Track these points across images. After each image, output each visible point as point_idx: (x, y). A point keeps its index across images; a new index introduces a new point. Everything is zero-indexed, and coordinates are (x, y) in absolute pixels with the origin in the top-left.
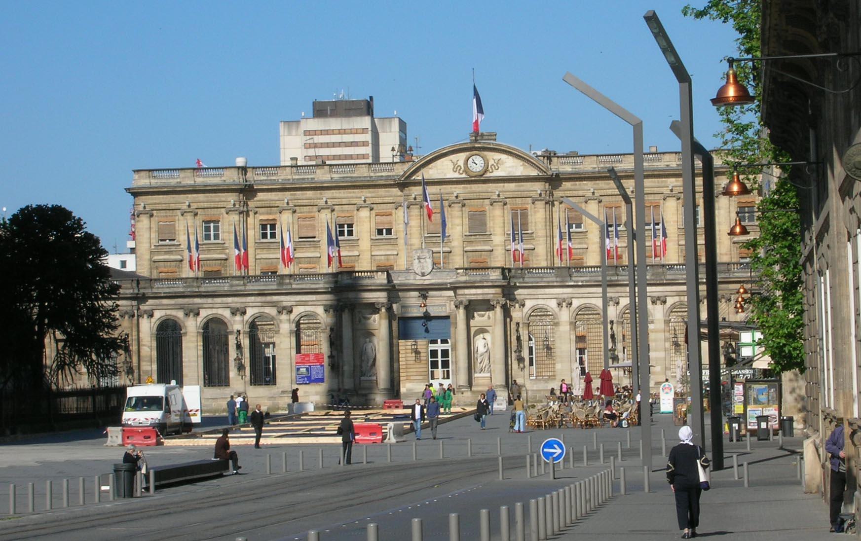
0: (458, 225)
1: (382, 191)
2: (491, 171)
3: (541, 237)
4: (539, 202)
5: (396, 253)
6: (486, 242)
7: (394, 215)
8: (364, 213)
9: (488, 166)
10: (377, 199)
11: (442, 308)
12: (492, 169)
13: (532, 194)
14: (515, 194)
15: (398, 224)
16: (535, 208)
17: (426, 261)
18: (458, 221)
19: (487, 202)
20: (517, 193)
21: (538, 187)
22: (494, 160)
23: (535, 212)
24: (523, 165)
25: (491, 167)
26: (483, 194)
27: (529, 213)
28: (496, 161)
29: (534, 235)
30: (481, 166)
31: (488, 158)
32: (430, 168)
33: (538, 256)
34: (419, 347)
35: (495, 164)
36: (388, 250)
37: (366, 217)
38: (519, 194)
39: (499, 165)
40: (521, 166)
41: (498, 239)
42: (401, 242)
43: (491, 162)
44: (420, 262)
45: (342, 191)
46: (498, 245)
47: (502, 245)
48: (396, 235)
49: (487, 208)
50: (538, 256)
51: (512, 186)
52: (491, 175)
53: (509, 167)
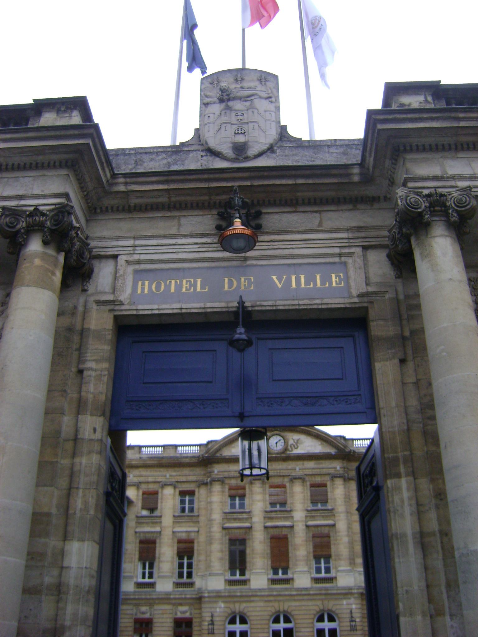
0: (259, 501)
1: (186, 471)
2: (290, 449)
3: (341, 513)
4: (338, 479)
5: (196, 529)
6: (286, 519)
7: (196, 493)
8: (168, 491)
9: (288, 444)
10: (181, 477)
11: (326, 278)
12: (292, 448)
13: (332, 471)
14: (314, 472)
15: (201, 502)
16: (334, 484)
17: (252, 107)
18: (258, 497)
19: (286, 480)
20: (316, 470)
21: (337, 466)
22: (294, 440)
23: (333, 488)
24: (322, 444)
25: (291, 446)
26: (284, 471)
27: (329, 490)
28: (296, 441)
29: (334, 511)
30: (281, 445)
31: (288, 437)
32: (234, 447)
33: (339, 532)
34: (216, 627)
35: (295, 444)
36: (190, 526)
37: (170, 495)
38: (318, 471)
39: (299, 445)
40: (319, 445)
41: (299, 515)
42: (202, 519)
43: (291, 442)
44: (228, 108)
45: (149, 470)
46: (298, 521)
47: (302, 521)
48: (198, 512)
49: (288, 485)
50: (339, 532)
51: (311, 464)
52: (291, 452)
53: (308, 446)
